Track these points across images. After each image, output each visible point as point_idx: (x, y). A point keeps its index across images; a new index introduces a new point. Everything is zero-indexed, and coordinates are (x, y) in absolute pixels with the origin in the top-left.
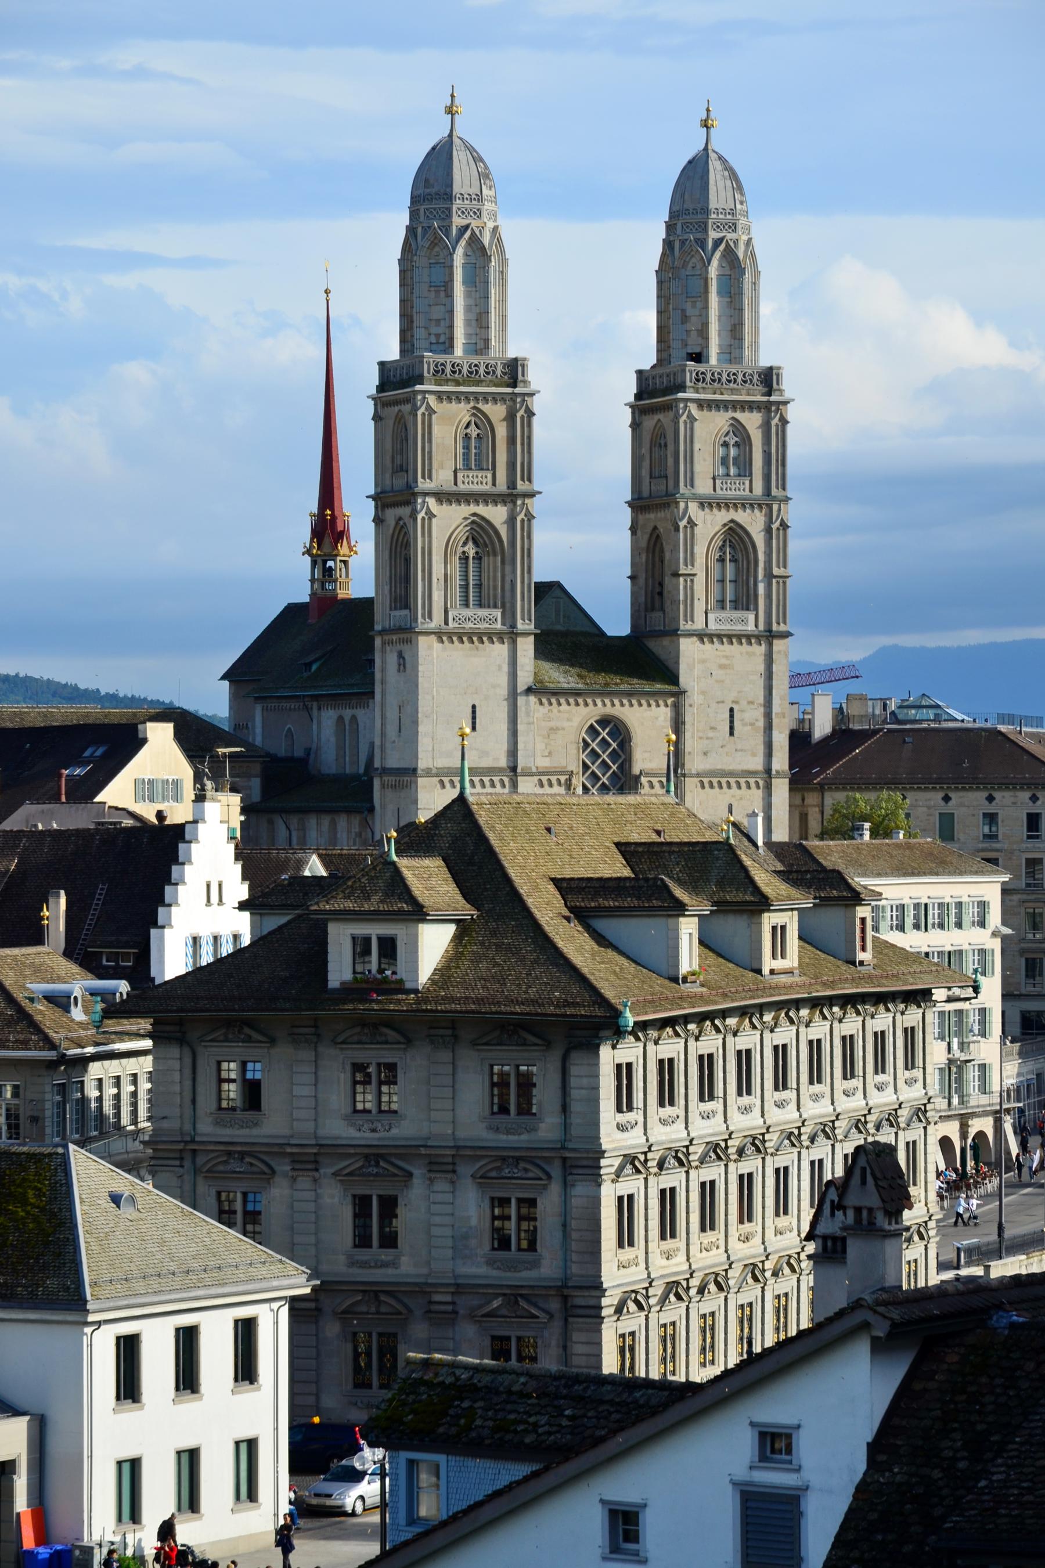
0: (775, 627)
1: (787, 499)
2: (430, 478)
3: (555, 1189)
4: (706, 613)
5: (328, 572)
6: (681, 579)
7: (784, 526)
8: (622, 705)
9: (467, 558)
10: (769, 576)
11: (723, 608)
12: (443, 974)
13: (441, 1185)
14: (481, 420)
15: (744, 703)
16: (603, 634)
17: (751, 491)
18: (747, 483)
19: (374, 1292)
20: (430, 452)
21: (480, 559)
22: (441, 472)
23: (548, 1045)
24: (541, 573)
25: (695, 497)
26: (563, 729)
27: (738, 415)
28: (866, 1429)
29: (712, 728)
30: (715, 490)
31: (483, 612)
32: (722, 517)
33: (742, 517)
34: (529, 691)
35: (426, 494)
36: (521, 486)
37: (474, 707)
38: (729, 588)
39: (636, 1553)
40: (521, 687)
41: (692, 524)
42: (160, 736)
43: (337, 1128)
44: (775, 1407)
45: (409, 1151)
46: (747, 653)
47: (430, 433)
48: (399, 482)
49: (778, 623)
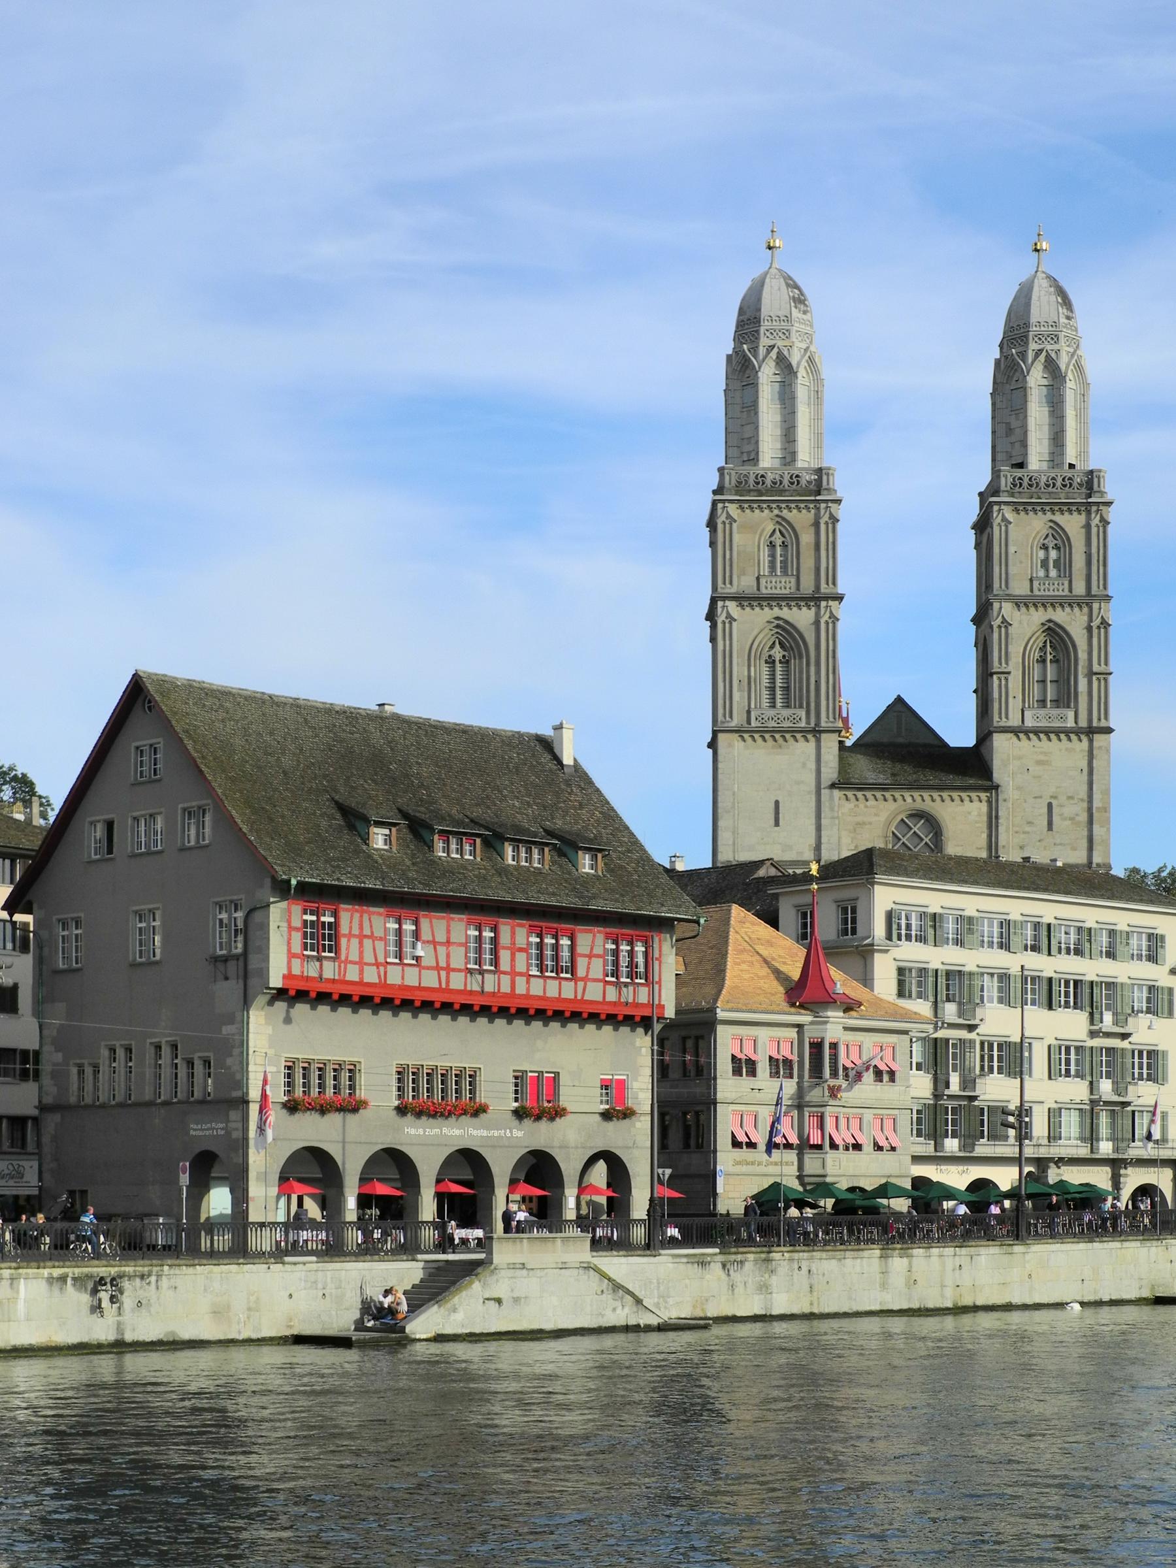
0: (1095, 724)
1: (1108, 598)
2: (731, 583)
4: (1023, 711)
6: (995, 677)
7: (1105, 624)
8: (933, 801)
9: (774, 661)
10: (1091, 674)
11: (1045, 707)
14: (786, 528)
15: (1063, 799)
16: (946, 745)
17: (1070, 590)
18: (1066, 583)
20: (731, 559)
21: (787, 662)
22: (743, 578)
25: (1009, 598)
26: (870, 823)
29: (1029, 823)
30: (1032, 591)
31: (786, 713)
32: (1038, 617)
33: (1060, 616)
34: (833, 786)
35: (724, 599)
36: (824, 588)
37: (777, 803)
40: (825, 782)
41: (1006, 624)
46: (1067, 749)
47: (731, 541)
49: (1099, 719)
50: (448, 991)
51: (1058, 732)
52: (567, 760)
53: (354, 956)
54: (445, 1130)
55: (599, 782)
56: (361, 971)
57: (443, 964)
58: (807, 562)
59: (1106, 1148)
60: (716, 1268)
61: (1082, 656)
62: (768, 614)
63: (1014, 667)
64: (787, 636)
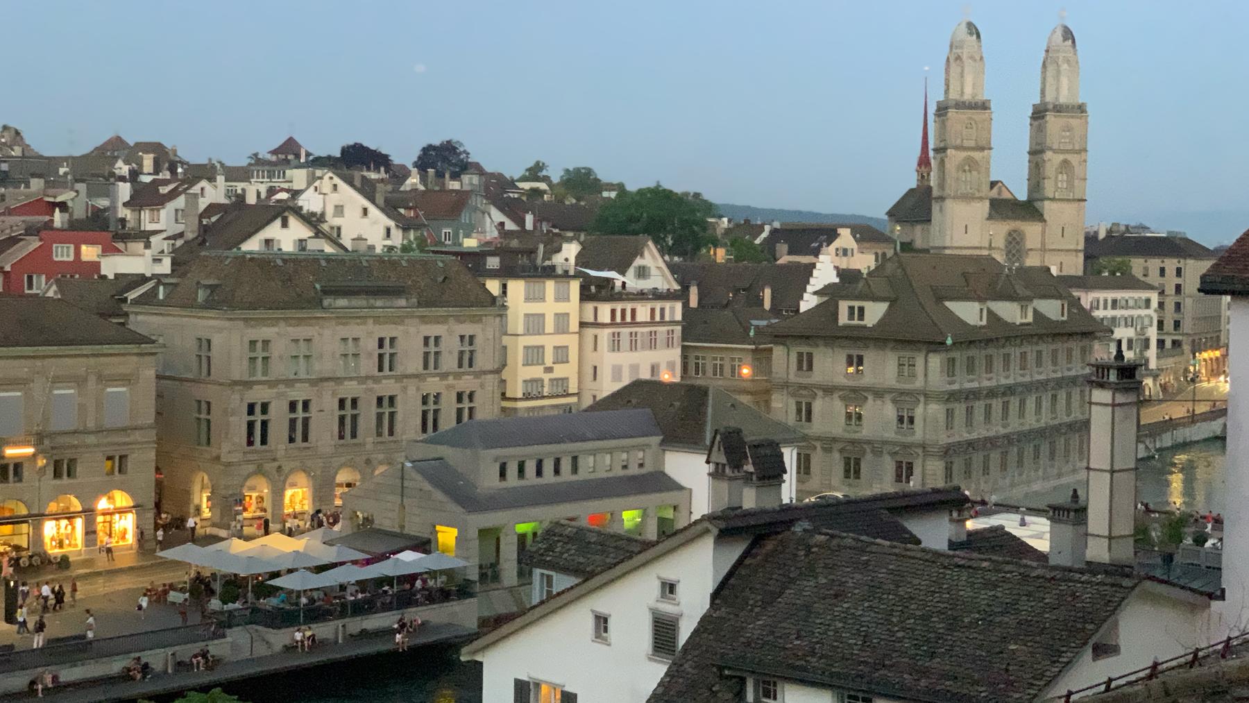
3: (921, 406)
5: (923, 177)
7: (1085, 161)
12: (882, 322)
13: (879, 402)
19: (853, 442)
23: (920, 350)
24: (993, 179)
28: (709, 587)
32: (1061, 157)
39: (606, 639)
42: (845, 233)
43: (842, 381)
44: (669, 568)
45: (867, 389)
48: (942, 145)
62: (964, 154)
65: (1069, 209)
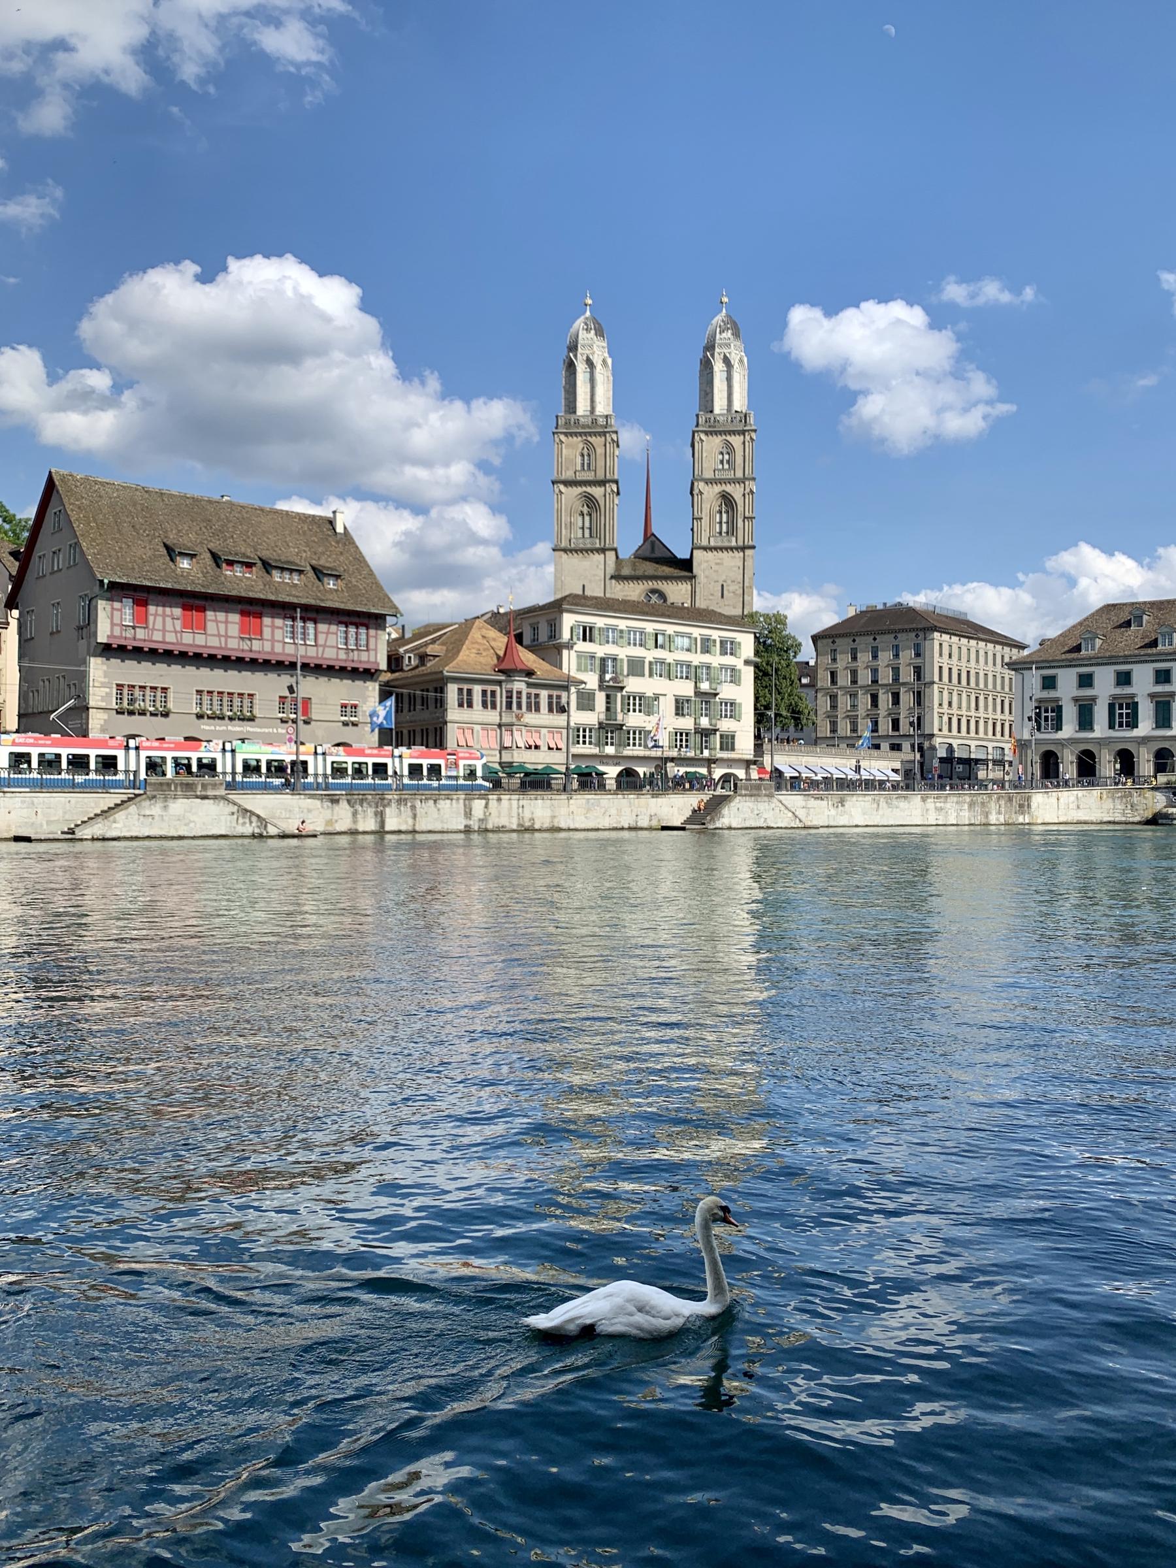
15: (729, 582)
27: (730, 438)
32: (718, 489)
33: (729, 488)
34: (612, 577)
38: (724, 526)
41: (701, 493)
50: (226, 648)
51: (726, 549)
52: (340, 529)
53: (159, 625)
54: (230, 728)
55: (358, 543)
56: (164, 636)
57: (222, 632)
58: (600, 463)
59: (706, 753)
60: (344, 804)
61: (740, 509)
62: (580, 490)
63: (705, 516)
64: (590, 501)
65: (732, 560)
